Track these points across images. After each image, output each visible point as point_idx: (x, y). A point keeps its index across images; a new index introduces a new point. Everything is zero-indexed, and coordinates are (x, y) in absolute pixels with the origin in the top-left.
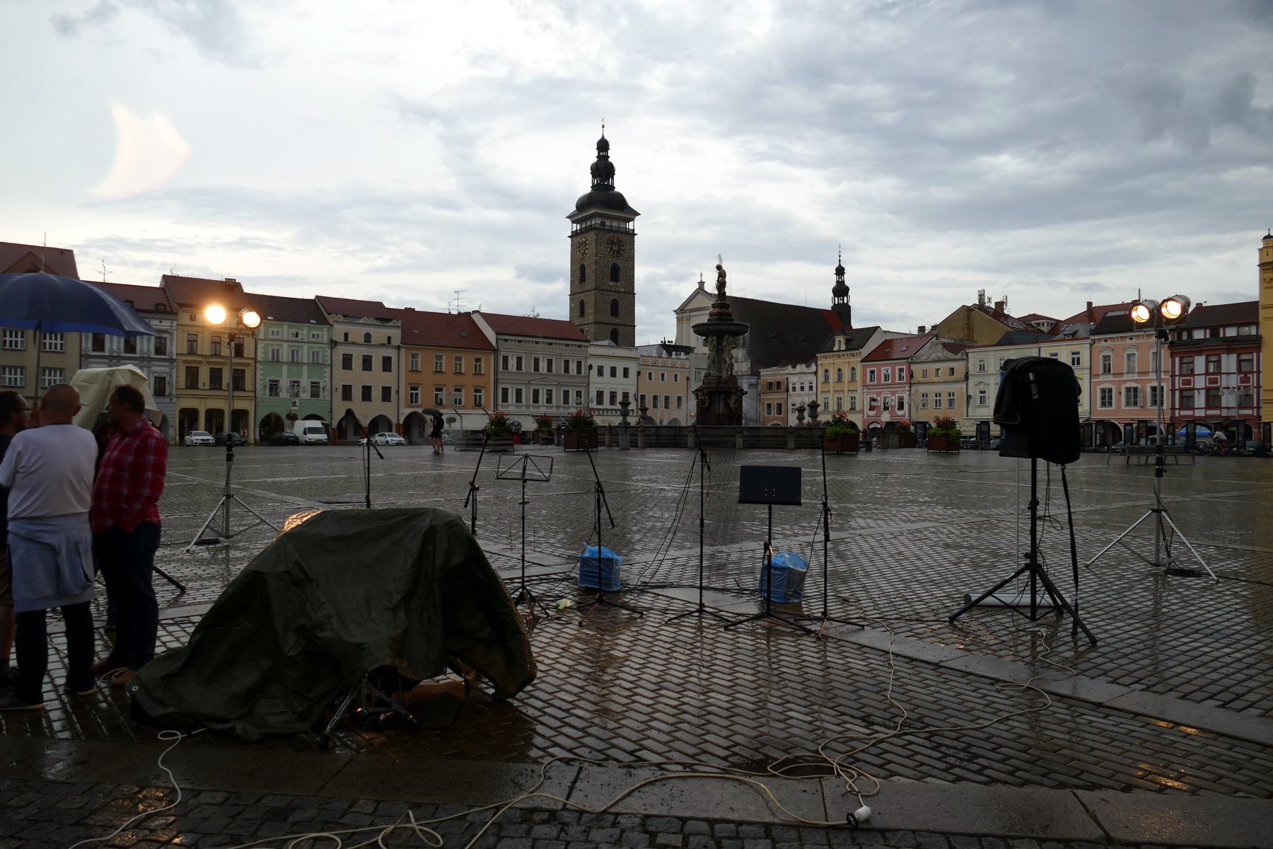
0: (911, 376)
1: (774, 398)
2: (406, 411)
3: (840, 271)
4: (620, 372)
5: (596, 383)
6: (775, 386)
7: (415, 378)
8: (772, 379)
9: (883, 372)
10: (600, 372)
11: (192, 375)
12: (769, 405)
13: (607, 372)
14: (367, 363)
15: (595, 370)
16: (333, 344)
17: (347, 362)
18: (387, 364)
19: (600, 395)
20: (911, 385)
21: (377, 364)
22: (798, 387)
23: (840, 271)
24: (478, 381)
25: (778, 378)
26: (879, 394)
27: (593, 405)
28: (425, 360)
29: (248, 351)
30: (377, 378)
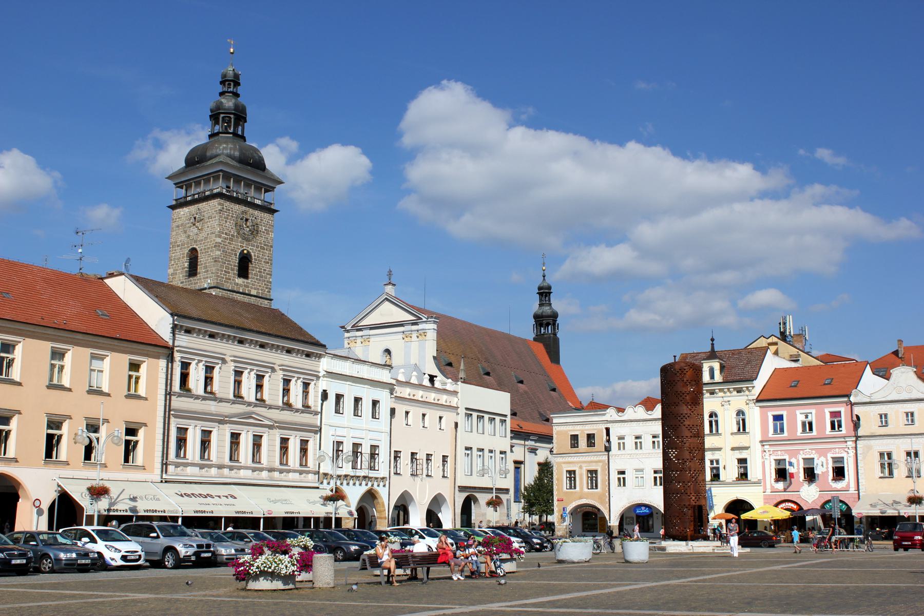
0: (856, 424)
1: (582, 462)
3: (545, 293)
4: (366, 406)
5: (339, 427)
6: (583, 442)
8: (576, 430)
9: (800, 418)
12: (572, 473)
13: (348, 404)
20: (857, 437)
22: (630, 442)
23: (545, 293)
25: (589, 429)
26: (794, 454)
27: (327, 467)
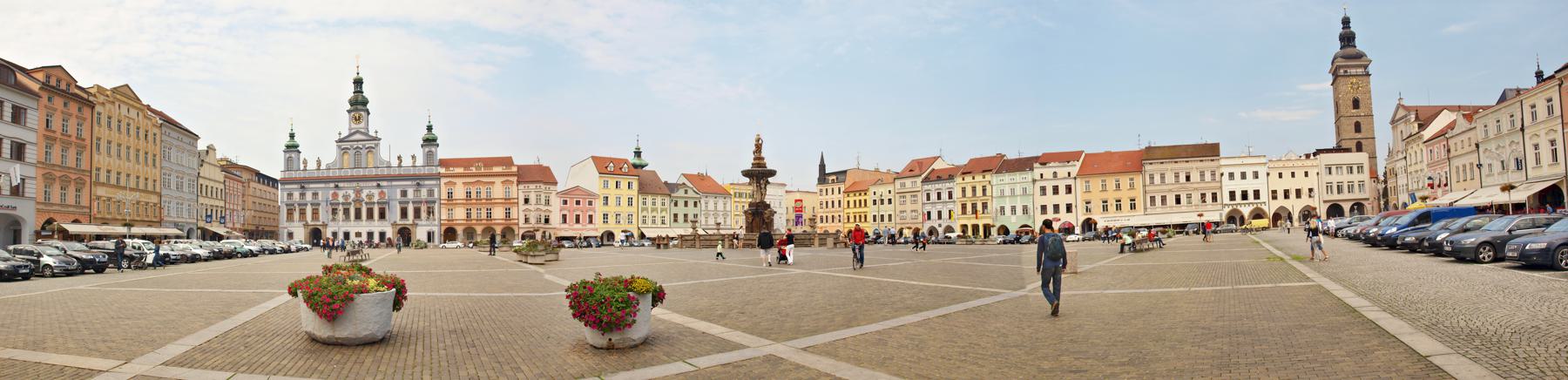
2: (1082, 219)
5: (1228, 186)
7: (1088, 197)
10: (1231, 175)
11: (964, 207)
13: (1237, 176)
14: (1056, 190)
15: (1226, 176)
16: (1034, 181)
17: (1043, 190)
18: (1069, 189)
19: (1232, 195)
21: (1062, 190)
24: (1132, 194)
28: (1096, 183)
29: (988, 192)
30: (1063, 199)
